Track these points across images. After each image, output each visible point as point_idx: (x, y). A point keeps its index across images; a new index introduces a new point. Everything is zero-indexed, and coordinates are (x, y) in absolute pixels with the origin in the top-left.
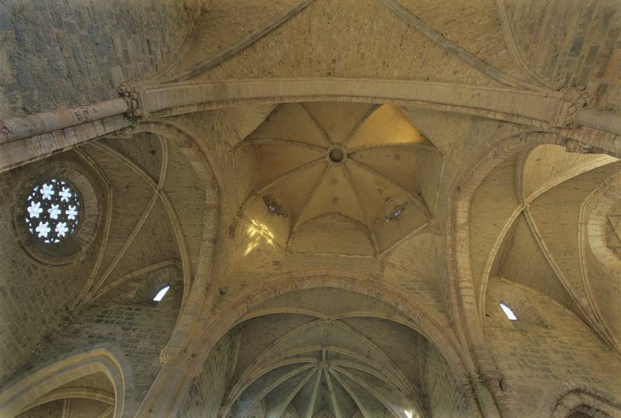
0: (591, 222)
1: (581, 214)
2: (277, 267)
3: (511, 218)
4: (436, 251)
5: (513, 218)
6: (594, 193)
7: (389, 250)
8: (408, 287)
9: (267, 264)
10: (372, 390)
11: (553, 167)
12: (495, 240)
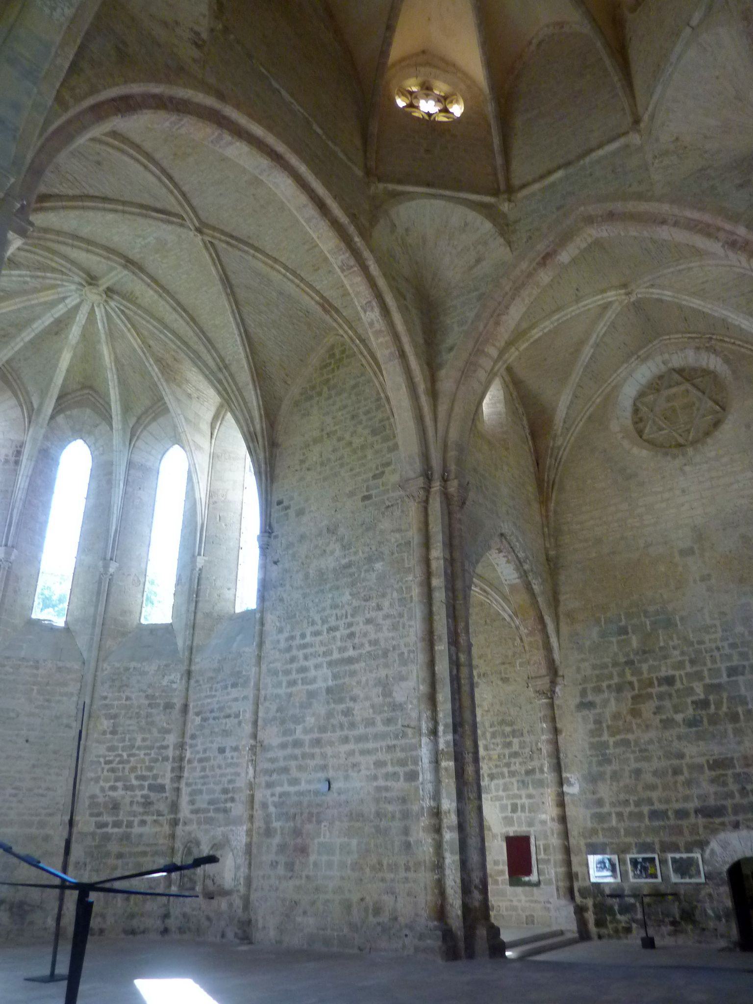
0: (650, 363)
1: (651, 345)
2: (195, 53)
3: (600, 297)
4: (478, 261)
5: (603, 299)
6: (689, 338)
7: (400, 188)
9: (177, 23)
10: (164, 384)
11: (707, 281)
12: (558, 309)
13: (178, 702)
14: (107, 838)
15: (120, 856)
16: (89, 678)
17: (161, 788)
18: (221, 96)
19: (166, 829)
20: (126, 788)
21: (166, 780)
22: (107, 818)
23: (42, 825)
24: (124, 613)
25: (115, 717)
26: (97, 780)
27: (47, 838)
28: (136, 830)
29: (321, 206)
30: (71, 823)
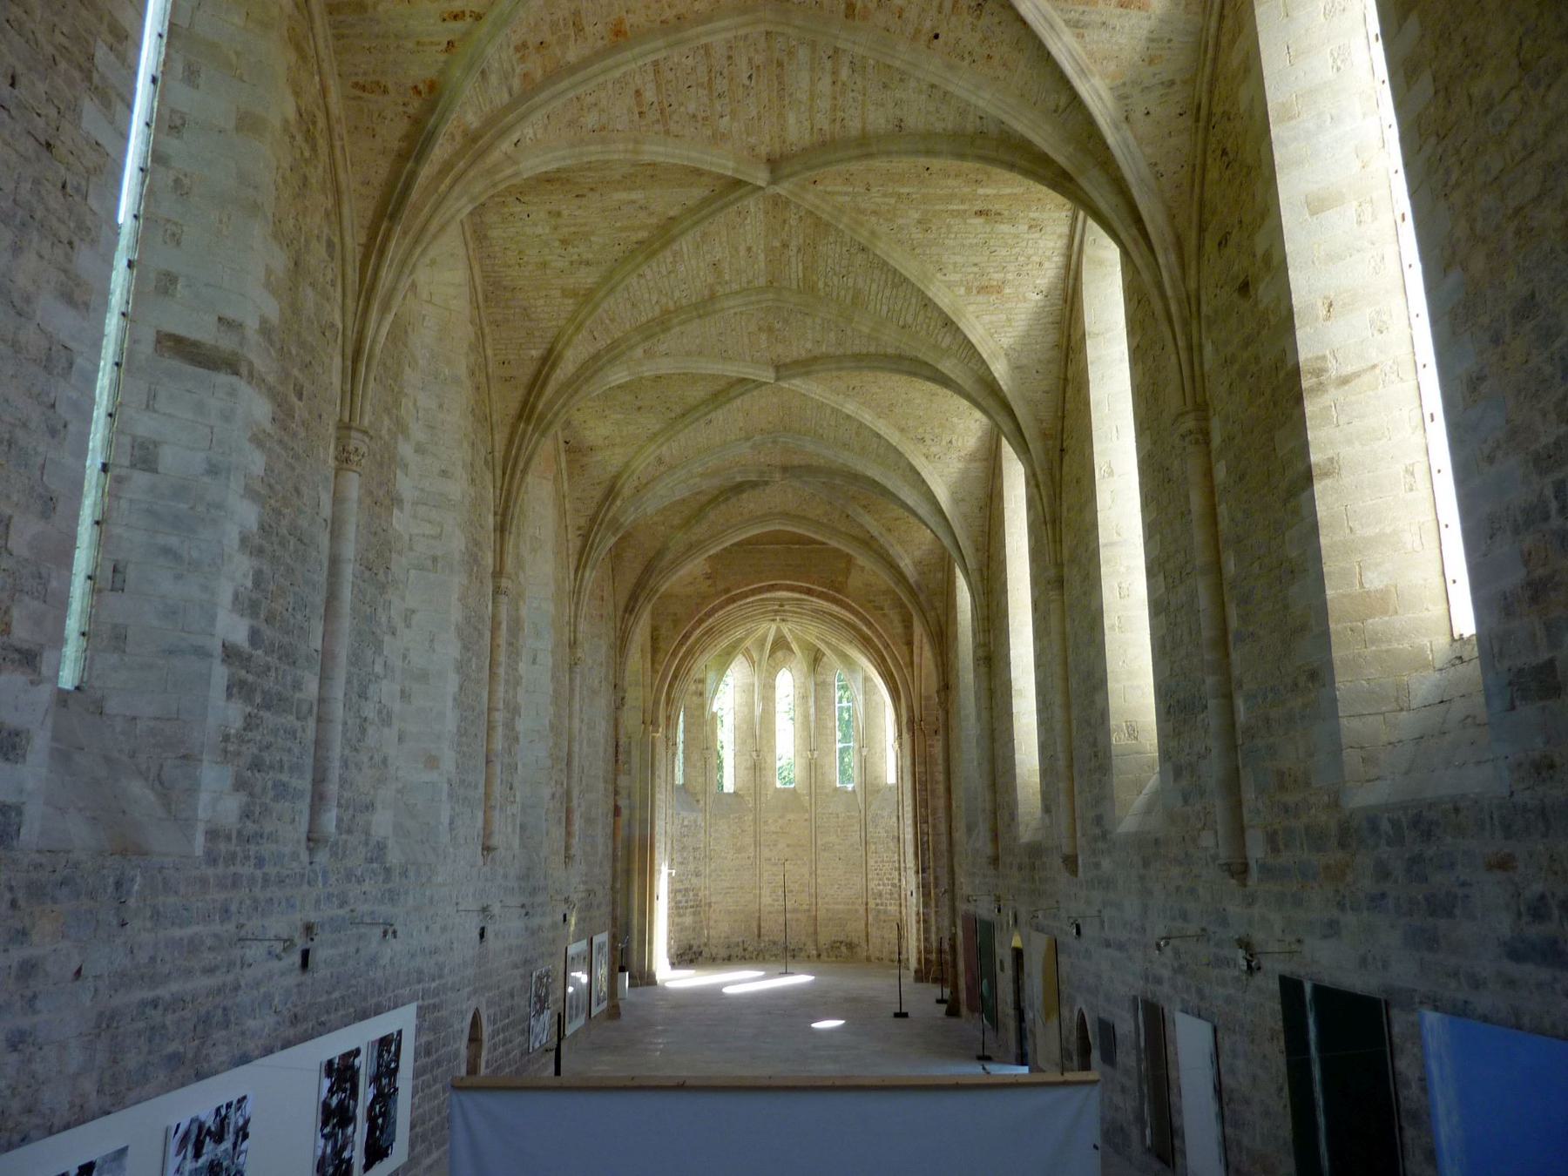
2: (709, 582)
8: (876, 604)
13: (896, 834)
14: (879, 911)
15: (885, 921)
16: (863, 822)
17: (894, 885)
18: (727, 590)
19: (897, 908)
20: (884, 885)
21: (897, 881)
22: (878, 901)
23: (853, 903)
24: (876, 778)
25: (875, 843)
26: (873, 879)
27: (857, 911)
28: (889, 908)
29: (809, 592)
30: (867, 904)
